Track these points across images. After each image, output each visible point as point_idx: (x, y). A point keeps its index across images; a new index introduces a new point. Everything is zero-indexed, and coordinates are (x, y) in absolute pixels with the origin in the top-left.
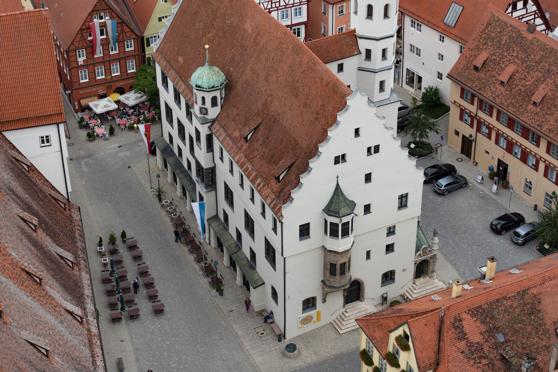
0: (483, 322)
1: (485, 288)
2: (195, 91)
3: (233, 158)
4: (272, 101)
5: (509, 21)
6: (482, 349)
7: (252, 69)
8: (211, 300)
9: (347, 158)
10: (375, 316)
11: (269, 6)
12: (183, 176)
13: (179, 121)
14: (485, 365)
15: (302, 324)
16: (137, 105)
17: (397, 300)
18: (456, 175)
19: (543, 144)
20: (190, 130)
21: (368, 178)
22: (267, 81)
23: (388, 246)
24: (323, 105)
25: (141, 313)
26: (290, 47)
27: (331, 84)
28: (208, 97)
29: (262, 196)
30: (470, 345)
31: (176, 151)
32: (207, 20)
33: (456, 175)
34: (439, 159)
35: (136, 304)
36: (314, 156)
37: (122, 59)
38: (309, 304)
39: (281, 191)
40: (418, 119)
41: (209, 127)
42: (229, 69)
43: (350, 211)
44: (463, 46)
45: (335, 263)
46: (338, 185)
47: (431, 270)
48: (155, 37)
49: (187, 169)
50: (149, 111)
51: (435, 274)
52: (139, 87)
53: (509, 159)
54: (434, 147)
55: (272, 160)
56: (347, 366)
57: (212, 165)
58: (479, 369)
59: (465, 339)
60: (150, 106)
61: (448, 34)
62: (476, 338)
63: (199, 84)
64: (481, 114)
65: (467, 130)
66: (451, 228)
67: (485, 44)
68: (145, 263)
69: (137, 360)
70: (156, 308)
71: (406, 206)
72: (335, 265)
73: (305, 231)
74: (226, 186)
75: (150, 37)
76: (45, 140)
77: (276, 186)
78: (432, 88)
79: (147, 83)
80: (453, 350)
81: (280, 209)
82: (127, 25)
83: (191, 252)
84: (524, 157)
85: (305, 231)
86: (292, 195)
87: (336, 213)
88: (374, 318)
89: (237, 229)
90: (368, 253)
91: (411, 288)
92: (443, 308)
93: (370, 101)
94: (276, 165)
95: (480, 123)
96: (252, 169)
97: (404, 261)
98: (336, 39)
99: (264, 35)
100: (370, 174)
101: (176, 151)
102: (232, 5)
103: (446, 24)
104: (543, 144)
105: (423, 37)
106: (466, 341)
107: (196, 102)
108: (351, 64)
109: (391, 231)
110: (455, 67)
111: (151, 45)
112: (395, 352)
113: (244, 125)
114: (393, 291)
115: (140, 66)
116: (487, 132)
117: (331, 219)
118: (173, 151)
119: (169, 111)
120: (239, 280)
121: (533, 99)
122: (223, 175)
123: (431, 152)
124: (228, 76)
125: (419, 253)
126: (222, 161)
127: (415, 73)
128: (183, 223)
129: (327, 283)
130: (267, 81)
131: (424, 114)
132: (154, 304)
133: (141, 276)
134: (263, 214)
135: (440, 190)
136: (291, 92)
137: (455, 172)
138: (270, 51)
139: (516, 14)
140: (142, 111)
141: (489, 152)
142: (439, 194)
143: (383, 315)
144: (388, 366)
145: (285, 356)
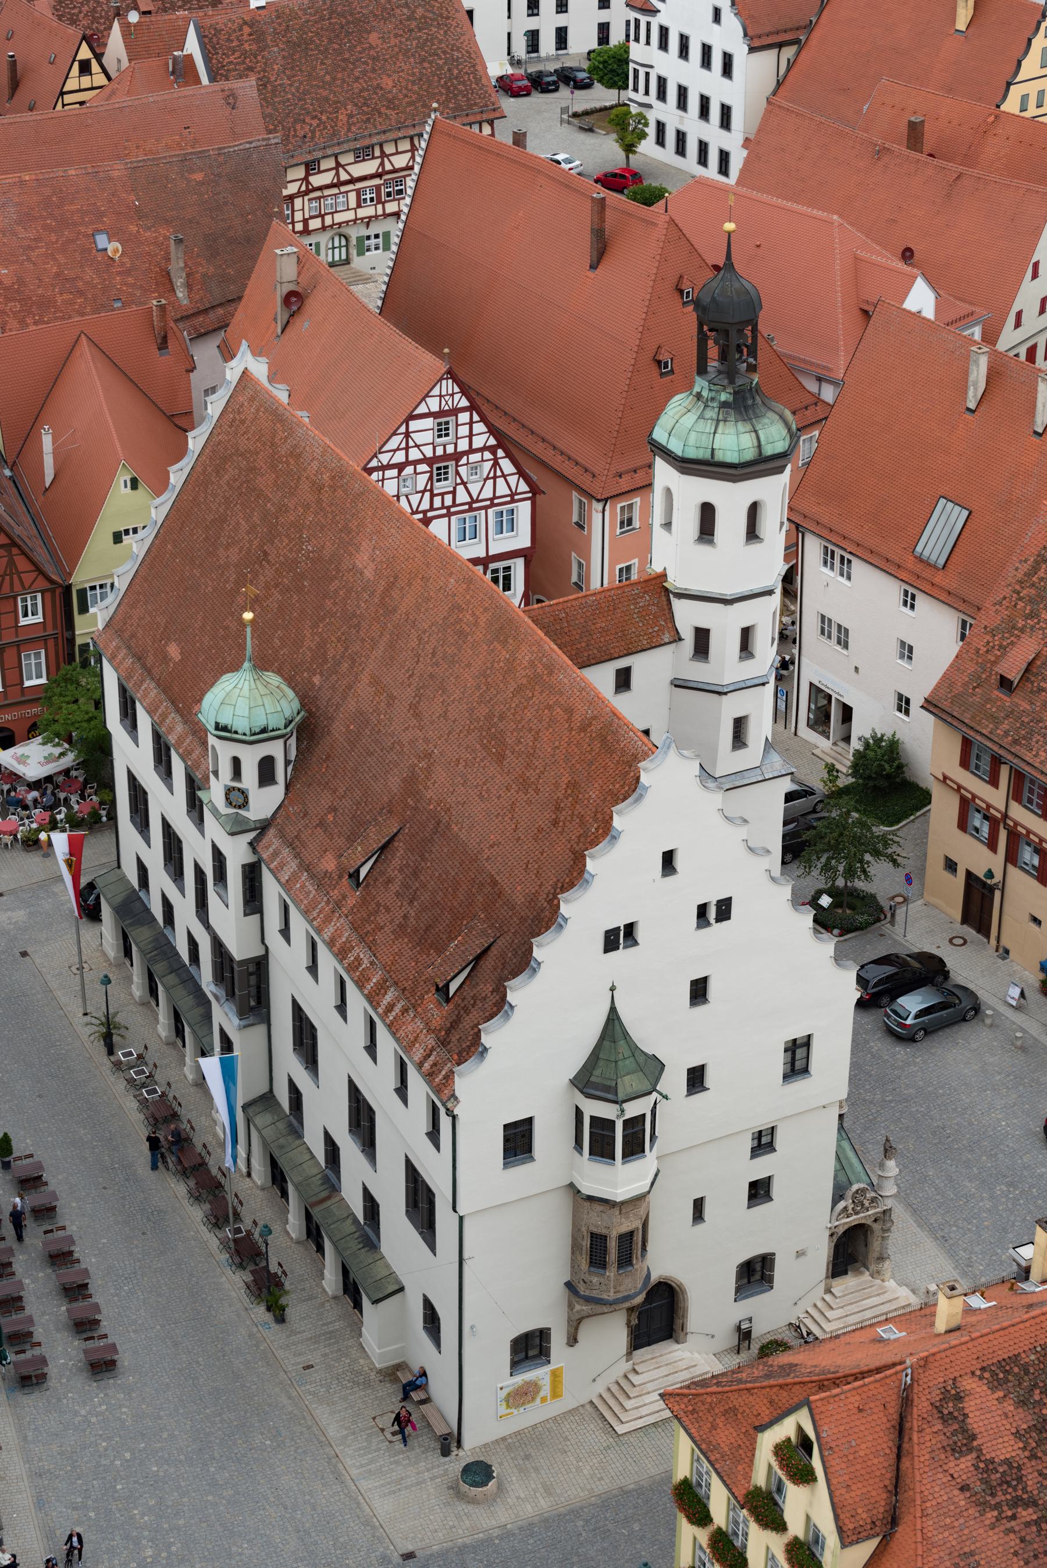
0: (1022, 1403)
1: (1030, 1306)
2: (212, 740)
3: (319, 931)
4: (428, 770)
6: (1019, 1479)
7: (375, 681)
8: (251, 1336)
9: (640, 934)
10: (718, 1384)
11: (425, 505)
12: (177, 981)
13: (166, 826)
14: (1028, 1524)
15: (508, 1406)
16: (49, 779)
17: (779, 1337)
18: (948, 985)
20: (196, 850)
21: (699, 991)
22: (417, 715)
23: (753, 1185)
24: (573, 785)
25: (52, 1370)
26: (483, 620)
27: (596, 726)
28: (250, 758)
29: (398, 1040)
31: (157, 910)
32: (250, 541)
33: (948, 985)
34: (900, 938)
35: (39, 1344)
36: (547, 928)
38: (530, 1348)
39: (454, 1025)
40: (841, 826)
41: (251, 844)
42: (310, 681)
43: (647, 1086)
44: (970, 621)
45: (604, 1231)
46: (613, 1010)
47: (876, 1255)
48: (101, 586)
49: (187, 963)
50: (83, 797)
51: (887, 1262)
52: (56, 727)
54: (885, 904)
55: (429, 939)
56: (636, 1527)
57: (261, 952)
58: (1012, 1536)
59: (970, 1450)
60: (86, 782)
61: (927, 587)
62: (1002, 1447)
63: (223, 721)
64: (1019, 814)
65: (980, 859)
66: (934, 1133)
67: (1031, 616)
68: (63, 1228)
69: (40, 1504)
70: (95, 1357)
71: (805, 1070)
72: (604, 1238)
73: (518, 1140)
74: (298, 1012)
75: (87, 586)
77: (437, 1012)
78: (881, 739)
79: (79, 716)
80: (937, 1483)
81: (449, 1077)
82: (23, 553)
83: (196, 1198)
85: (518, 1140)
86: (485, 1039)
87: (607, 1089)
88: (714, 1389)
89: (327, 1134)
90: (699, 1206)
91: (820, 1304)
92: (908, 1362)
93: (706, 774)
94: (440, 951)
95: (1015, 838)
96: (372, 963)
97: (800, 1227)
98: (611, 601)
99: (410, 585)
100: (705, 980)
101: (157, 910)
102: (319, 501)
103: (920, 559)
105: (855, 596)
106: (974, 1455)
107: (216, 773)
108: (653, 668)
109: (763, 1143)
110: (947, 680)
111: (92, 610)
112: (774, 1488)
113: (352, 839)
114: (769, 1313)
115: (58, 668)
116: (1036, 861)
118: (147, 910)
119: (139, 797)
120: (331, 1280)
122: (289, 980)
123: (879, 920)
124: (306, 700)
125: (842, 1204)
126: (288, 939)
127: (834, 696)
128: (175, 1116)
129: (582, 1289)
130: (417, 715)
131: (858, 811)
132: (90, 1344)
133: (53, 1264)
134: (402, 1091)
135: (903, 1026)
136: (484, 747)
137: (946, 975)
138: (425, 632)
140: (62, 796)
142: (899, 1038)
143: (740, 1381)
144: (754, 1528)
145: (460, 1496)
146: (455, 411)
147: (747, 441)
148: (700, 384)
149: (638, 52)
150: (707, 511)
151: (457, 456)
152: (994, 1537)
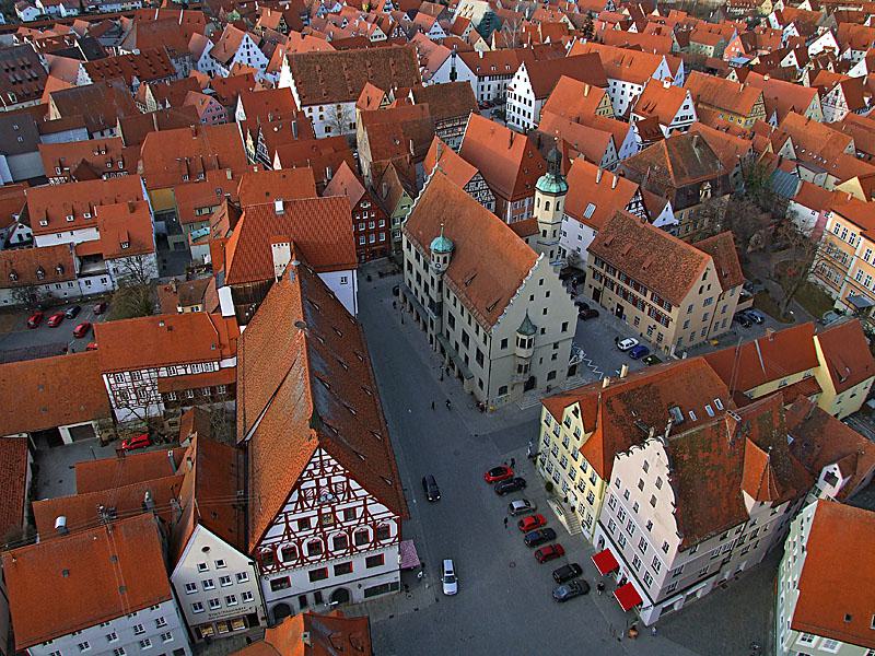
19: (649, 294)
20: (426, 277)
37: (377, 231)
38: (503, 390)
53: (625, 303)
64: (608, 275)
65: (598, 285)
73: (504, 344)
76: (344, 280)
84: (635, 302)
85: (504, 344)
104: (649, 294)
105: (571, 225)
117: (521, 336)
121: (644, 265)
141: (611, 298)
148: (547, 174)
149: (509, 100)
150: (548, 203)
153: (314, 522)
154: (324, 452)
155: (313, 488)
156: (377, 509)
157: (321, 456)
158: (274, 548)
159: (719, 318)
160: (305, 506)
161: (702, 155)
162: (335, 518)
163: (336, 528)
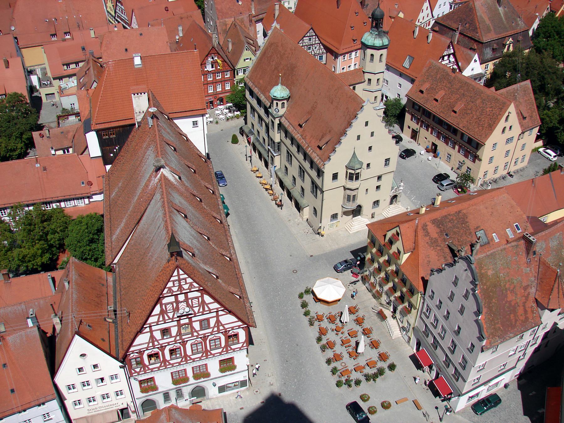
5: (441, 67)
21: (370, 148)
24: (347, 108)
30: (431, 239)
31: (256, 133)
38: (334, 216)
43: (360, 167)
65: (415, 126)
73: (335, 176)
76: (195, 124)
80: (423, 241)
85: (335, 176)
97: (385, 195)
117: (350, 171)
130: (314, 94)
139: (443, 63)
146: (312, 36)
147: (381, 42)
150: (372, 55)
151: (312, 45)
152: (433, 252)
153: (174, 331)
154: (181, 272)
155: (172, 303)
156: (228, 319)
157: (179, 275)
158: (141, 353)
159: (519, 154)
160: (167, 318)
161: (506, 14)
162: (192, 328)
163: (193, 336)
